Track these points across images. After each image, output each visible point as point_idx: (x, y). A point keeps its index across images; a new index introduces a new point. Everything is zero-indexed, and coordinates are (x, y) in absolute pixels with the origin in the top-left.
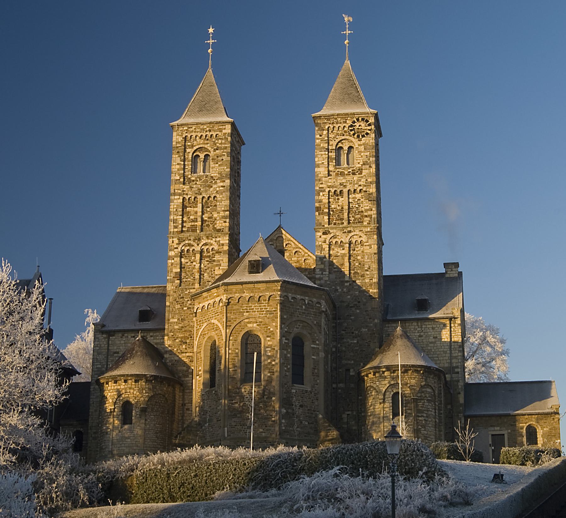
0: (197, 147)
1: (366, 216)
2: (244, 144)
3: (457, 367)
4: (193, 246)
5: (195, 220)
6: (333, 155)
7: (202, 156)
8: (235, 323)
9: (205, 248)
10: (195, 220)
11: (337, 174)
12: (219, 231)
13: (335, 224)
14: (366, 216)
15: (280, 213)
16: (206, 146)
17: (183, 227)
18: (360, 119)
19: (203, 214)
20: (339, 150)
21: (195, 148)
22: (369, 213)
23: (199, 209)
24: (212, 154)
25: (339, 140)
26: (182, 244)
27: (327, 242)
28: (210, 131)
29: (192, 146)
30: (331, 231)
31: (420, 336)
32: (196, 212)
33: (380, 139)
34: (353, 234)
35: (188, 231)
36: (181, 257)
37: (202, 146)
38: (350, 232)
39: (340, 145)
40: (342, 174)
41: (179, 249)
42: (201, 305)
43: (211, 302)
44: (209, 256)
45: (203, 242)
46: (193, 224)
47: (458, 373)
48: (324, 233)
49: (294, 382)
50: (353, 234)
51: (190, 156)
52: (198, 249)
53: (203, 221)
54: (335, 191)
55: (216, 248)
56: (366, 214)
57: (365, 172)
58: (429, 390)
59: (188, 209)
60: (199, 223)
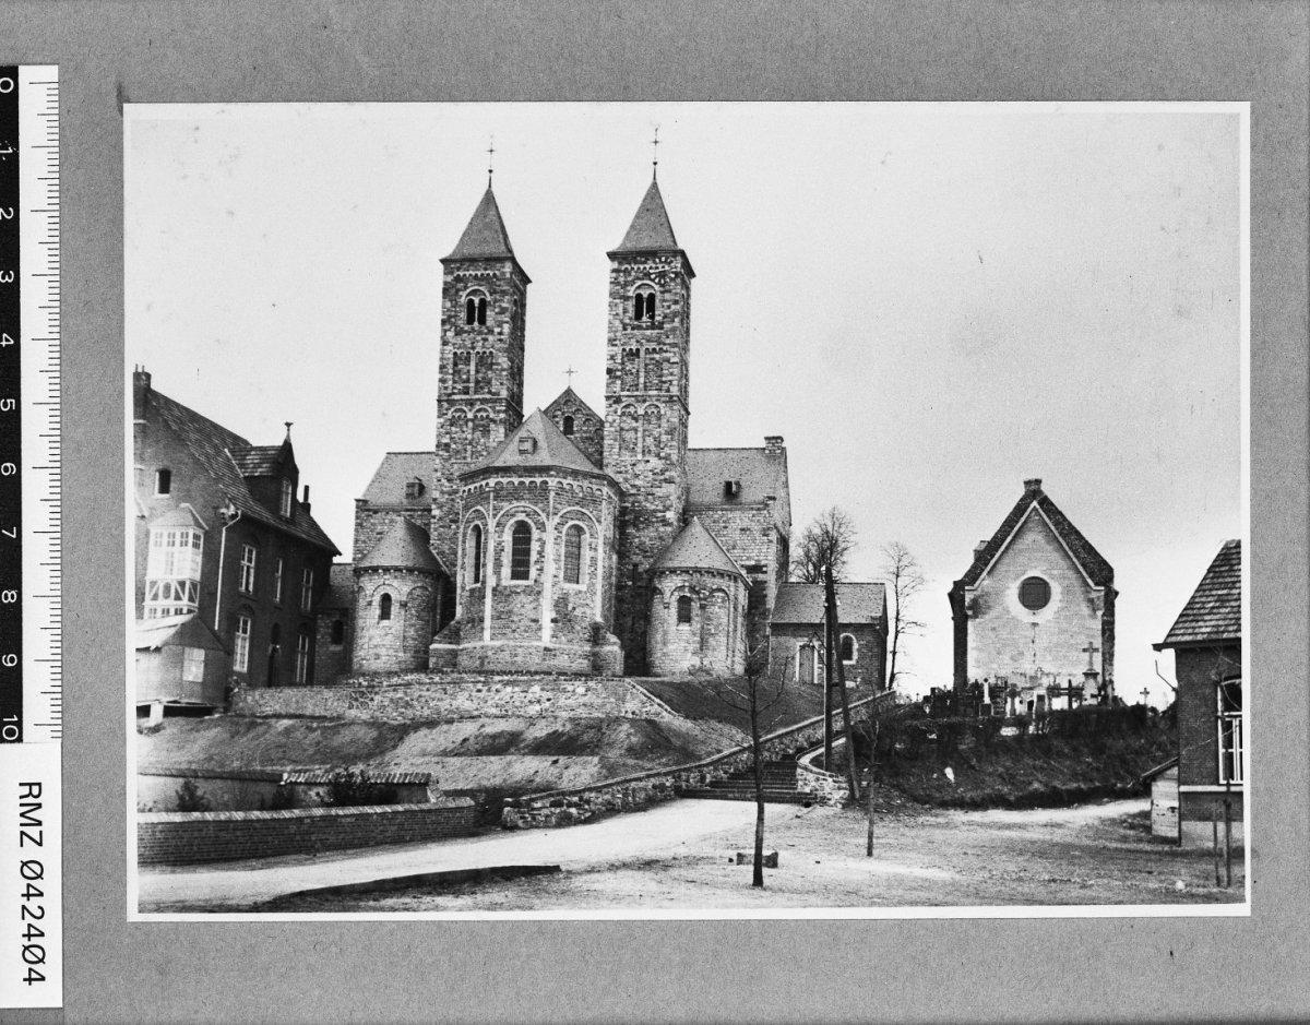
0: (471, 289)
1: (665, 382)
2: (530, 281)
3: (766, 566)
4: (465, 412)
5: (468, 381)
6: (631, 305)
7: (477, 301)
8: (502, 512)
9: (479, 415)
10: (468, 381)
11: (633, 329)
12: (494, 394)
13: (628, 390)
14: (665, 382)
15: (570, 372)
16: (481, 288)
17: (454, 388)
18: (663, 259)
19: (477, 372)
20: (639, 297)
21: (468, 291)
22: (670, 378)
23: (472, 367)
24: (489, 298)
25: (637, 285)
26: (453, 409)
27: (619, 413)
28: (486, 269)
29: (466, 288)
30: (624, 399)
31: (725, 527)
32: (469, 371)
33: (693, 281)
34: (647, 404)
35: (459, 393)
36: (452, 425)
37: (476, 287)
38: (645, 401)
39: (638, 292)
40: (639, 328)
41: (449, 416)
42: (466, 489)
43: (478, 485)
44: (483, 426)
45: (477, 407)
46: (465, 385)
47: (766, 572)
48: (615, 402)
49: (568, 579)
50: (647, 404)
51: (463, 298)
52: (470, 415)
53: (477, 382)
54: (631, 349)
55: (492, 415)
56: (664, 379)
57: (667, 326)
58: (721, 594)
59: (460, 366)
60: (472, 385)
